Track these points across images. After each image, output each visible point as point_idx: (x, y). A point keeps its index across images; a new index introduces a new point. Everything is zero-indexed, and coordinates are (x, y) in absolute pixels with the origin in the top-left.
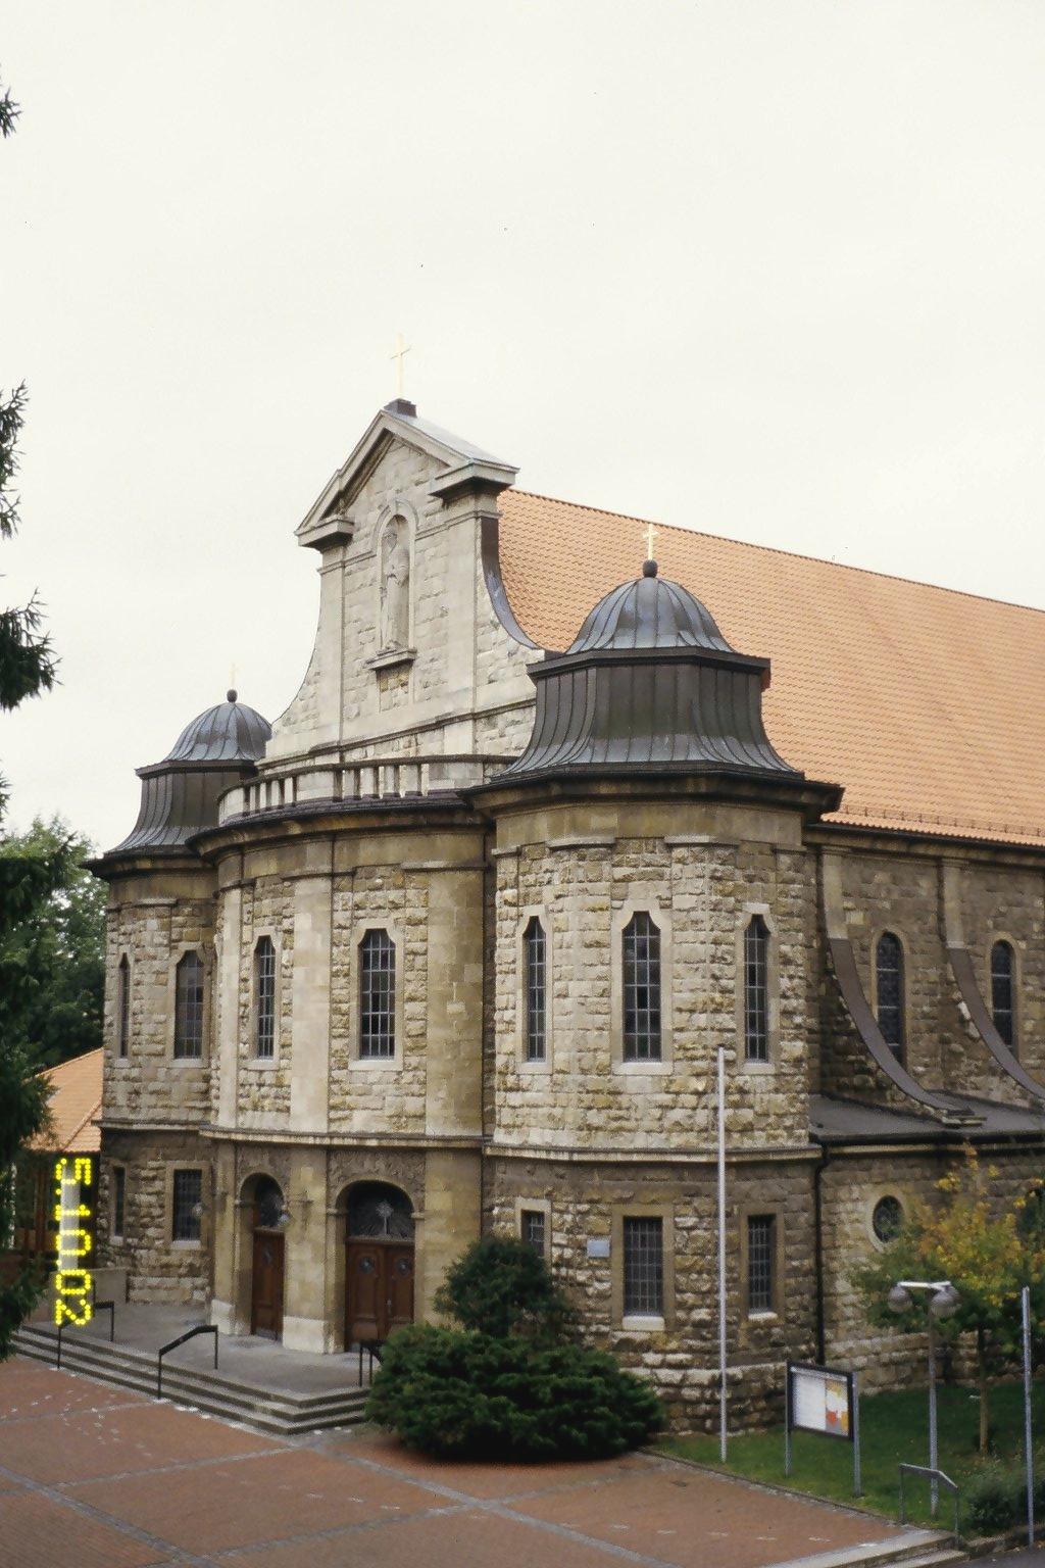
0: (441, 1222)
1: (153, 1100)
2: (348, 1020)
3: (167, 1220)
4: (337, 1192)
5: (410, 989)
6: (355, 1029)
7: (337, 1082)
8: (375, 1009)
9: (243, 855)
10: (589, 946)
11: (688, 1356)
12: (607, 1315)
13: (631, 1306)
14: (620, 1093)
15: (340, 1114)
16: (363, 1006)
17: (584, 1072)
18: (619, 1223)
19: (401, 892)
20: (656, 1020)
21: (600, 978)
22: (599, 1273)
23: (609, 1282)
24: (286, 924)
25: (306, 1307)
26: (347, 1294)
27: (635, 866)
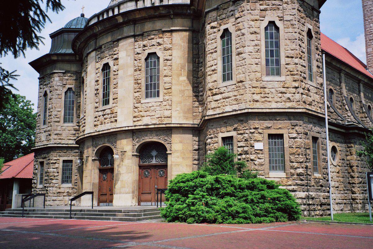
0: (178, 154)
1: (56, 137)
2: (141, 86)
3: (60, 177)
4: (136, 147)
5: (165, 73)
6: (144, 88)
7: (136, 108)
8: (151, 81)
9: (96, 39)
12: (263, 172)
13: (273, 168)
14: (265, 88)
15: (138, 119)
16: (147, 81)
17: (251, 80)
18: (266, 136)
19: (162, 39)
21: (256, 45)
22: (259, 156)
23: (265, 159)
24: (115, 57)
25: (123, 190)
26: (139, 183)
27: (268, 5)
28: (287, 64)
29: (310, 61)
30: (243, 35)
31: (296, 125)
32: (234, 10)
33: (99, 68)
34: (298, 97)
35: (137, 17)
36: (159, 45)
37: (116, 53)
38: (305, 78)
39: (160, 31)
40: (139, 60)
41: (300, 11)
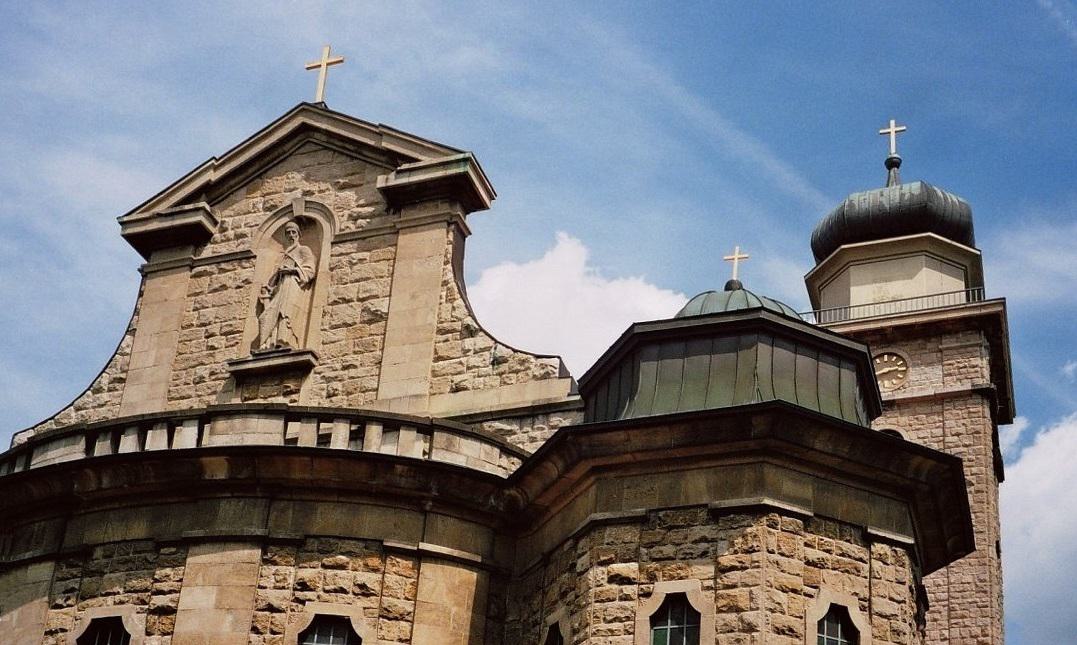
10: (779, 631)
24: (159, 601)
27: (828, 551)
30: (750, 628)
32: (714, 540)
33: (63, 630)
35: (297, 475)
36: (364, 595)
37: (164, 586)
39: (374, 547)
40: (273, 632)
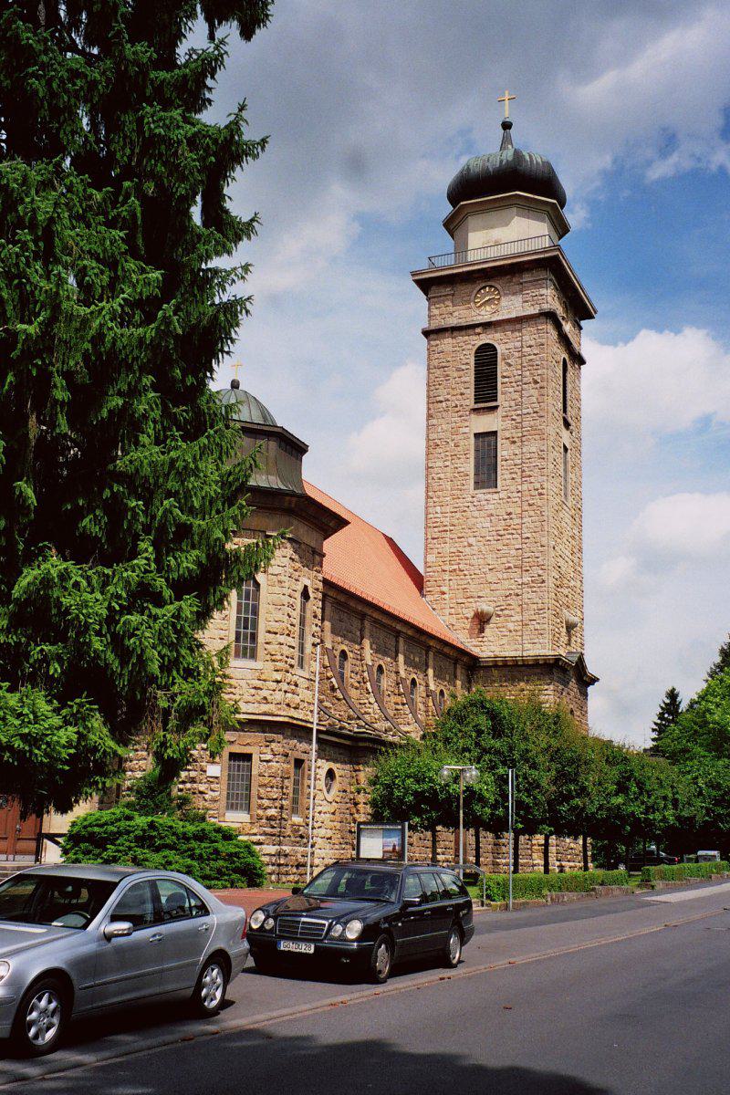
11: (263, 837)
20: (254, 637)
22: (212, 786)
23: (220, 792)
28: (267, 643)
29: (302, 636)
31: (273, 741)
34: (279, 696)
38: (292, 666)
41: (293, 560)
